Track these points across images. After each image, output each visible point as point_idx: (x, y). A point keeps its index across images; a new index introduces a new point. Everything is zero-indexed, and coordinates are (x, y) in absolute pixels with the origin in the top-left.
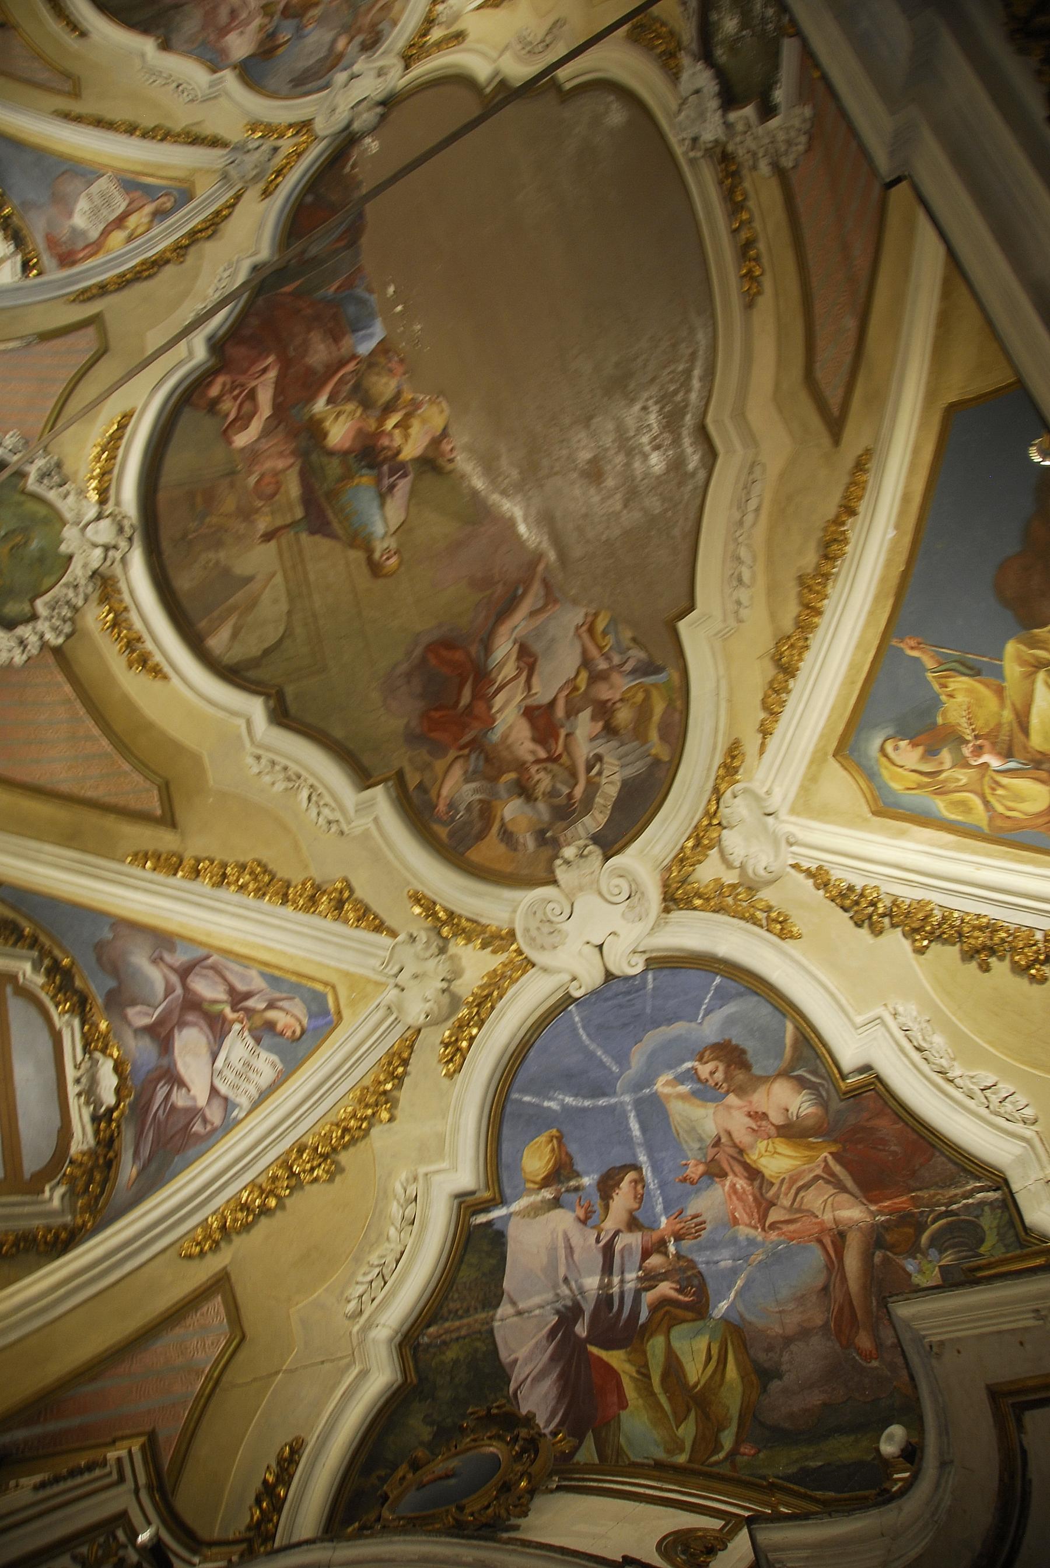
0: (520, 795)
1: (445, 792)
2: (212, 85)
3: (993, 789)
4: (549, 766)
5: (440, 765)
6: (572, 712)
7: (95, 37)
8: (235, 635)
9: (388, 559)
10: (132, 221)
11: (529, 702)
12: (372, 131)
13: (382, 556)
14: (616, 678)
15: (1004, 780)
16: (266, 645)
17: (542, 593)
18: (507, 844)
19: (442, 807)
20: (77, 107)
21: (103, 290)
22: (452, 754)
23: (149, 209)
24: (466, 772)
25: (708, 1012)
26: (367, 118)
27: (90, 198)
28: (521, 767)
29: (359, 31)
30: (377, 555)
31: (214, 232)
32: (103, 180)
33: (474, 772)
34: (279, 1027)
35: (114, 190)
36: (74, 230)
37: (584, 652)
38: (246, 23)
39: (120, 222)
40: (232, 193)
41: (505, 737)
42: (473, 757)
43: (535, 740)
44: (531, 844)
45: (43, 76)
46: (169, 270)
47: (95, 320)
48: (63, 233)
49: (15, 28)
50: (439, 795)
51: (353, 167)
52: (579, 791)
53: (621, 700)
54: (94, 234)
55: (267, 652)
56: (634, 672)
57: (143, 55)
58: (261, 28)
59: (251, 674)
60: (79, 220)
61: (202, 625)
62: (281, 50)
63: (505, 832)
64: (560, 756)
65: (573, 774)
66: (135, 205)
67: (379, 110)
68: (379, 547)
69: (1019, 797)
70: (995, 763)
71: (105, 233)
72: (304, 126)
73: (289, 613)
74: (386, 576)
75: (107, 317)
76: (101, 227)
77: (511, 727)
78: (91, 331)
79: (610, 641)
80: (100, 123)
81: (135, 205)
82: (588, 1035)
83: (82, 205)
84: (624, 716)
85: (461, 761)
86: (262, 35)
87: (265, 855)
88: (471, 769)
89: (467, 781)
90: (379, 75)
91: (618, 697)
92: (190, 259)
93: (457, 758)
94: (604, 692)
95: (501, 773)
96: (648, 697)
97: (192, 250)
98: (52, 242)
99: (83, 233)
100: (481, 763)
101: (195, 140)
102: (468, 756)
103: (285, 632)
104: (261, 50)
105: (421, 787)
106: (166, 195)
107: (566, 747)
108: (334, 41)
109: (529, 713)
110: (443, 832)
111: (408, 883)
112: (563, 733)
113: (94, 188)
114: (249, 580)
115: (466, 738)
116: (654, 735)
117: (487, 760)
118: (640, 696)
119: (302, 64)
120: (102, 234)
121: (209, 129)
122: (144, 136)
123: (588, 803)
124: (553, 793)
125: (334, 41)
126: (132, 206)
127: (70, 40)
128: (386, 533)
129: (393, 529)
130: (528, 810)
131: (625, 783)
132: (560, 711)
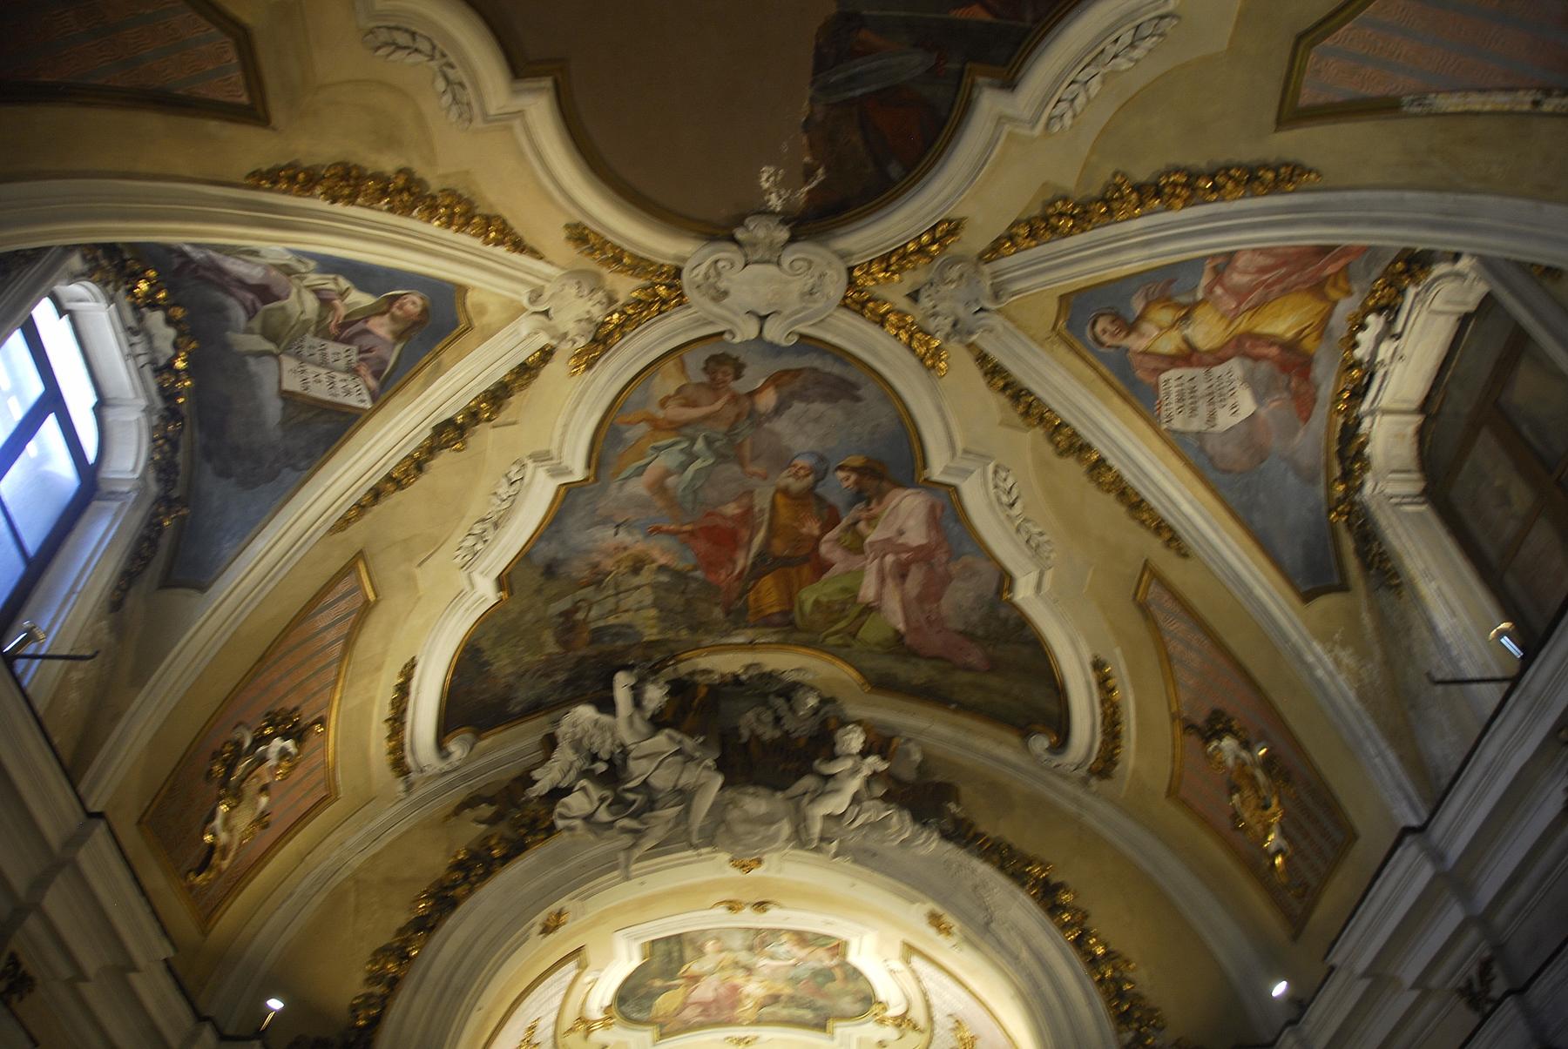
2: (966, 473)
7: (1088, 659)
10: (1169, 344)
12: (765, 212)
20: (1154, 548)
21: (1251, 178)
23: (1136, 343)
26: (758, 230)
27: (1212, 417)
29: (735, 398)
31: (1052, 203)
32: (1178, 423)
35: (1170, 404)
36: (1259, 398)
38: (888, 545)
39: (1188, 356)
40: (1004, 263)
45: (1176, 627)
46: (1142, 174)
47: (1291, 115)
48: (1277, 404)
49: (1174, 717)
51: (809, 173)
54: (1235, 368)
57: (1039, 586)
58: (872, 521)
60: (1246, 404)
62: (857, 461)
66: (1153, 364)
67: (740, 234)
71: (1218, 357)
72: (857, 302)
75: (1270, 116)
76: (1218, 370)
78: (1306, 98)
80: (1135, 504)
81: (1153, 364)
83: (1225, 420)
86: (875, 508)
90: (725, 294)
92: (1104, 174)
97: (1095, 191)
98: (1304, 405)
99: (1250, 380)
101: (1016, 394)
104: (885, 485)
106: (1102, 344)
108: (778, 410)
113: (1196, 425)
119: (832, 413)
120: (1222, 361)
121: (994, 403)
122: (1086, 448)
125: (778, 410)
126: (1163, 365)
127: (1119, 668)
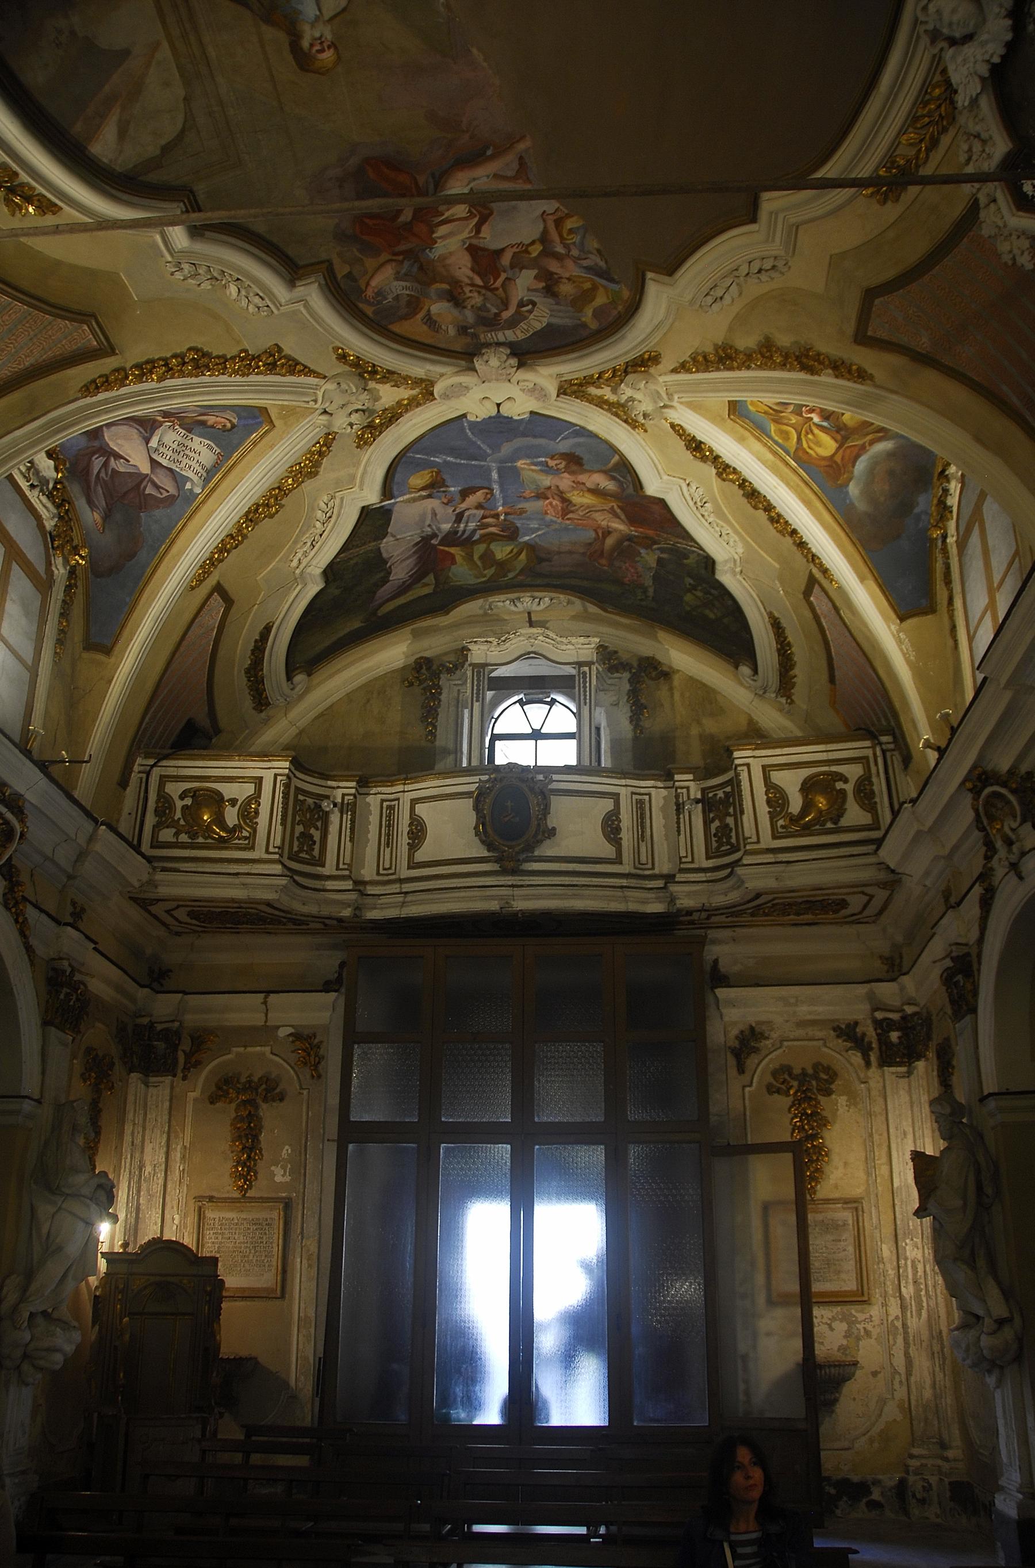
0: (449, 301)
1: (374, 283)
3: (807, 433)
4: (483, 291)
5: (370, 263)
6: (517, 264)
8: (122, 133)
9: (322, 51)
11: (475, 242)
13: (312, 45)
14: (569, 263)
15: (816, 431)
16: (163, 142)
17: (515, 166)
18: (430, 327)
19: (370, 293)
22: (384, 257)
24: (398, 273)
25: (563, 439)
28: (456, 283)
30: (305, 44)
33: (406, 275)
34: (209, 423)
37: (545, 232)
41: (443, 258)
42: (406, 264)
43: (472, 270)
44: (452, 331)
50: (368, 284)
52: (506, 315)
53: (569, 279)
55: (166, 149)
56: (588, 269)
59: (153, 177)
61: (78, 128)
63: (430, 318)
64: (497, 289)
65: (505, 304)
68: (308, 35)
69: (819, 444)
70: (816, 419)
73: (187, 99)
74: (317, 72)
77: (451, 254)
79: (577, 239)
82: (472, 433)
84: (566, 289)
85: (394, 264)
87: (198, 342)
88: (403, 271)
89: (397, 279)
91: (567, 275)
93: (391, 260)
94: (554, 266)
95: (434, 281)
96: (594, 288)
100: (415, 269)
102: (402, 262)
103: (185, 121)
105: (349, 276)
107: (503, 285)
109: (473, 250)
110: (369, 311)
111: (333, 343)
112: (503, 276)
114: (126, 53)
115: (402, 247)
116: (589, 312)
117: (421, 268)
118: (588, 285)
123: (513, 323)
124: (483, 308)
128: (317, 19)
129: (328, 14)
130: (455, 312)
131: (549, 325)
132: (506, 260)
